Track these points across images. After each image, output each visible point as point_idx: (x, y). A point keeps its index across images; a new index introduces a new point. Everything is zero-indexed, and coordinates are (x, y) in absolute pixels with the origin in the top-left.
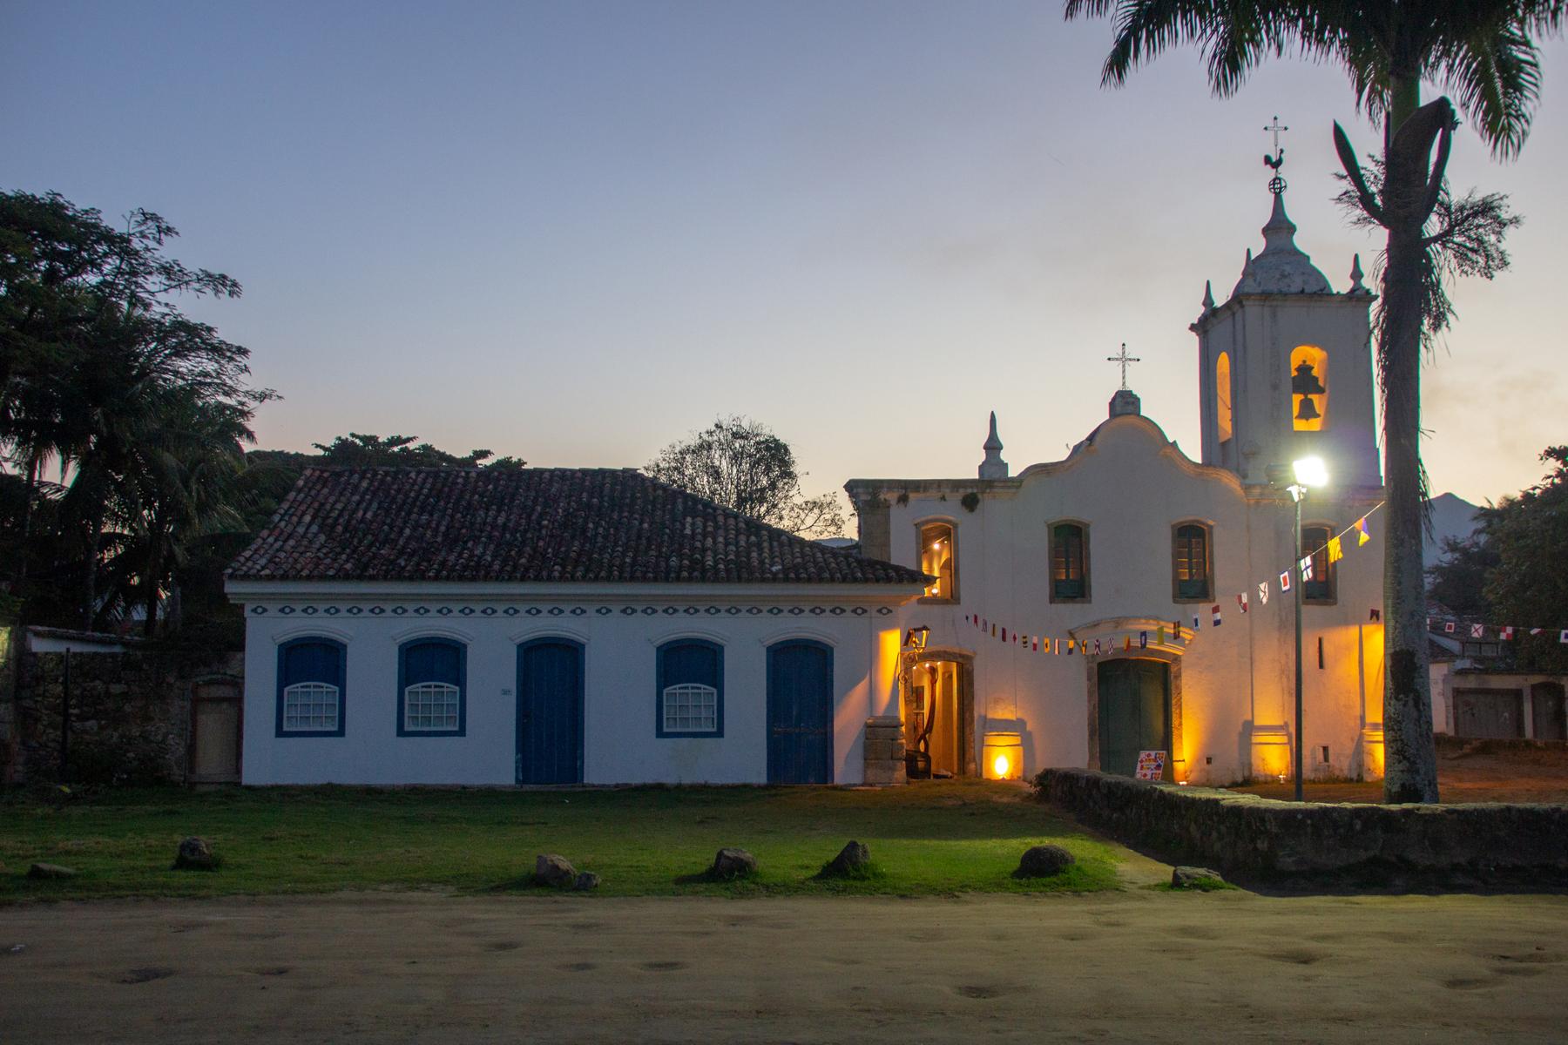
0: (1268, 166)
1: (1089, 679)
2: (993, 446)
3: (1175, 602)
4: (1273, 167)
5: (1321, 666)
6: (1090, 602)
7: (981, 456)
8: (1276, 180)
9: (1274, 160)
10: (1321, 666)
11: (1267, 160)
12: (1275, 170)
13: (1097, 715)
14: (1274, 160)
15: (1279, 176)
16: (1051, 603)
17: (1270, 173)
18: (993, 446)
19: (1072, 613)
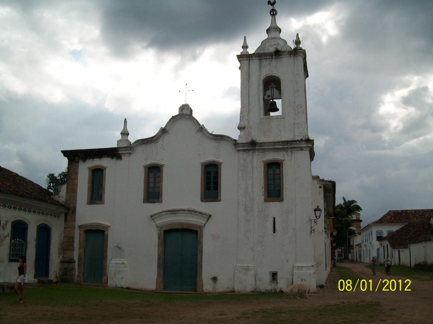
0: (270, 5)
1: (159, 238)
2: (125, 134)
3: (202, 201)
4: (271, 5)
5: (274, 232)
6: (161, 202)
7: (119, 137)
8: (273, 10)
9: (272, 2)
10: (274, 232)
11: (269, 3)
12: (272, 6)
13: (162, 256)
14: (272, 2)
15: (274, 8)
16: (144, 202)
17: (270, 7)
18: (125, 134)
19: (155, 208)
